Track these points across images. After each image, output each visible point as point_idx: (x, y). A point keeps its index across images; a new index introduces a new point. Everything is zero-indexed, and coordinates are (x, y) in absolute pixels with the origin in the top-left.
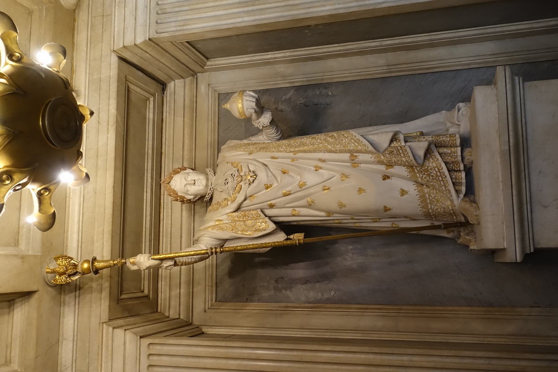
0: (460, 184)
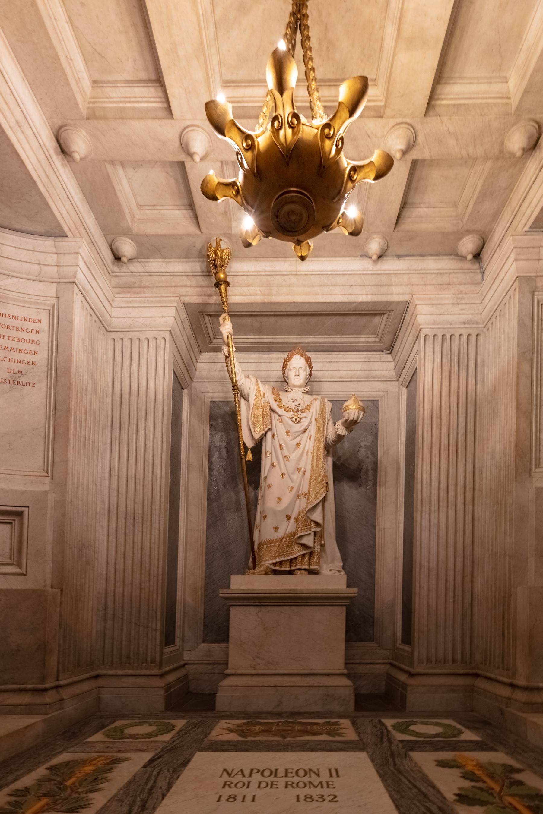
0: (281, 567)
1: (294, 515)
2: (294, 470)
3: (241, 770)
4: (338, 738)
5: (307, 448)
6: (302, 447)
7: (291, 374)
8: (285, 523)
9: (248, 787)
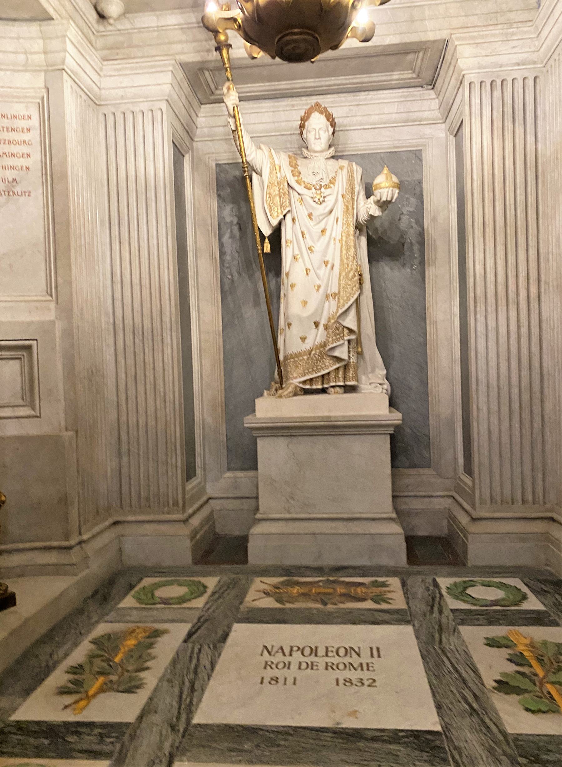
0: (311, 385)
1: (323, 322)
2: (320, 268)
3: (282, 648)
4: (384, 606)
5: (334, 235)
6: (328, 233)
7: (310, 136)
8: (314, 330)
9: (289, 668)
